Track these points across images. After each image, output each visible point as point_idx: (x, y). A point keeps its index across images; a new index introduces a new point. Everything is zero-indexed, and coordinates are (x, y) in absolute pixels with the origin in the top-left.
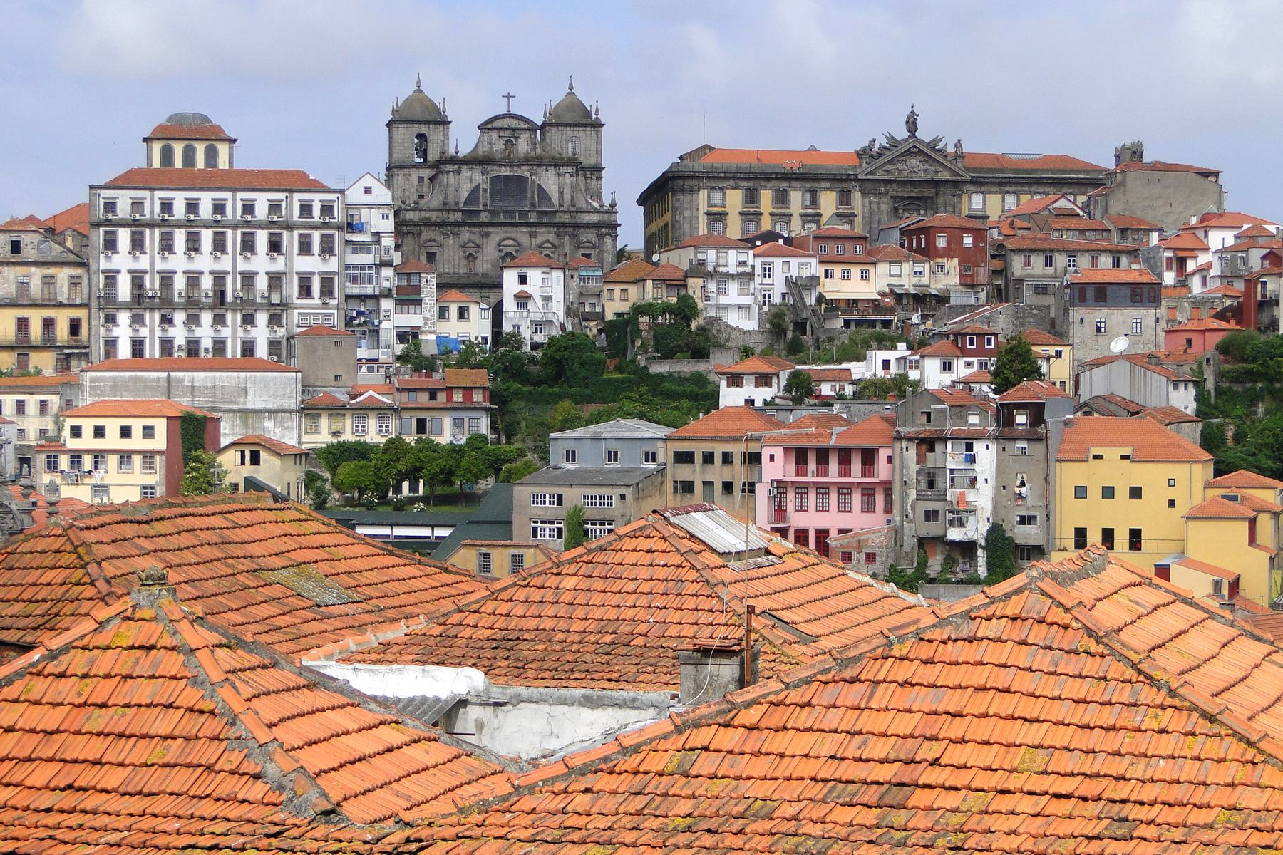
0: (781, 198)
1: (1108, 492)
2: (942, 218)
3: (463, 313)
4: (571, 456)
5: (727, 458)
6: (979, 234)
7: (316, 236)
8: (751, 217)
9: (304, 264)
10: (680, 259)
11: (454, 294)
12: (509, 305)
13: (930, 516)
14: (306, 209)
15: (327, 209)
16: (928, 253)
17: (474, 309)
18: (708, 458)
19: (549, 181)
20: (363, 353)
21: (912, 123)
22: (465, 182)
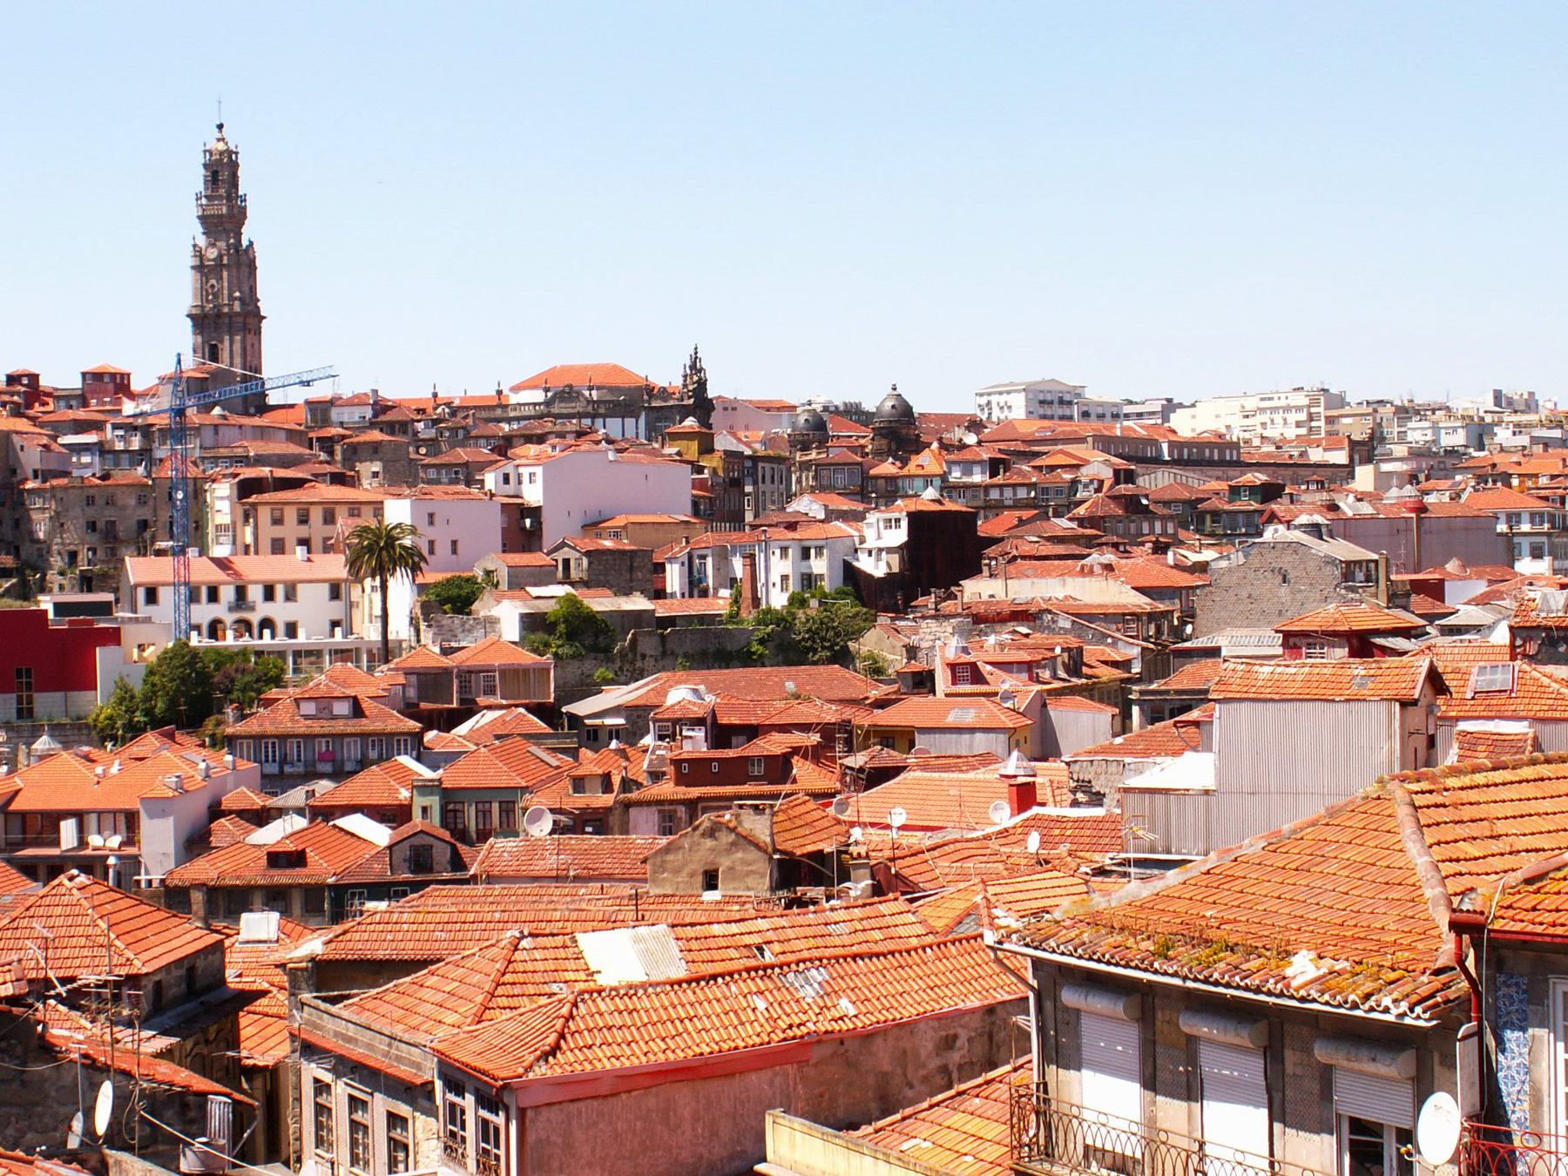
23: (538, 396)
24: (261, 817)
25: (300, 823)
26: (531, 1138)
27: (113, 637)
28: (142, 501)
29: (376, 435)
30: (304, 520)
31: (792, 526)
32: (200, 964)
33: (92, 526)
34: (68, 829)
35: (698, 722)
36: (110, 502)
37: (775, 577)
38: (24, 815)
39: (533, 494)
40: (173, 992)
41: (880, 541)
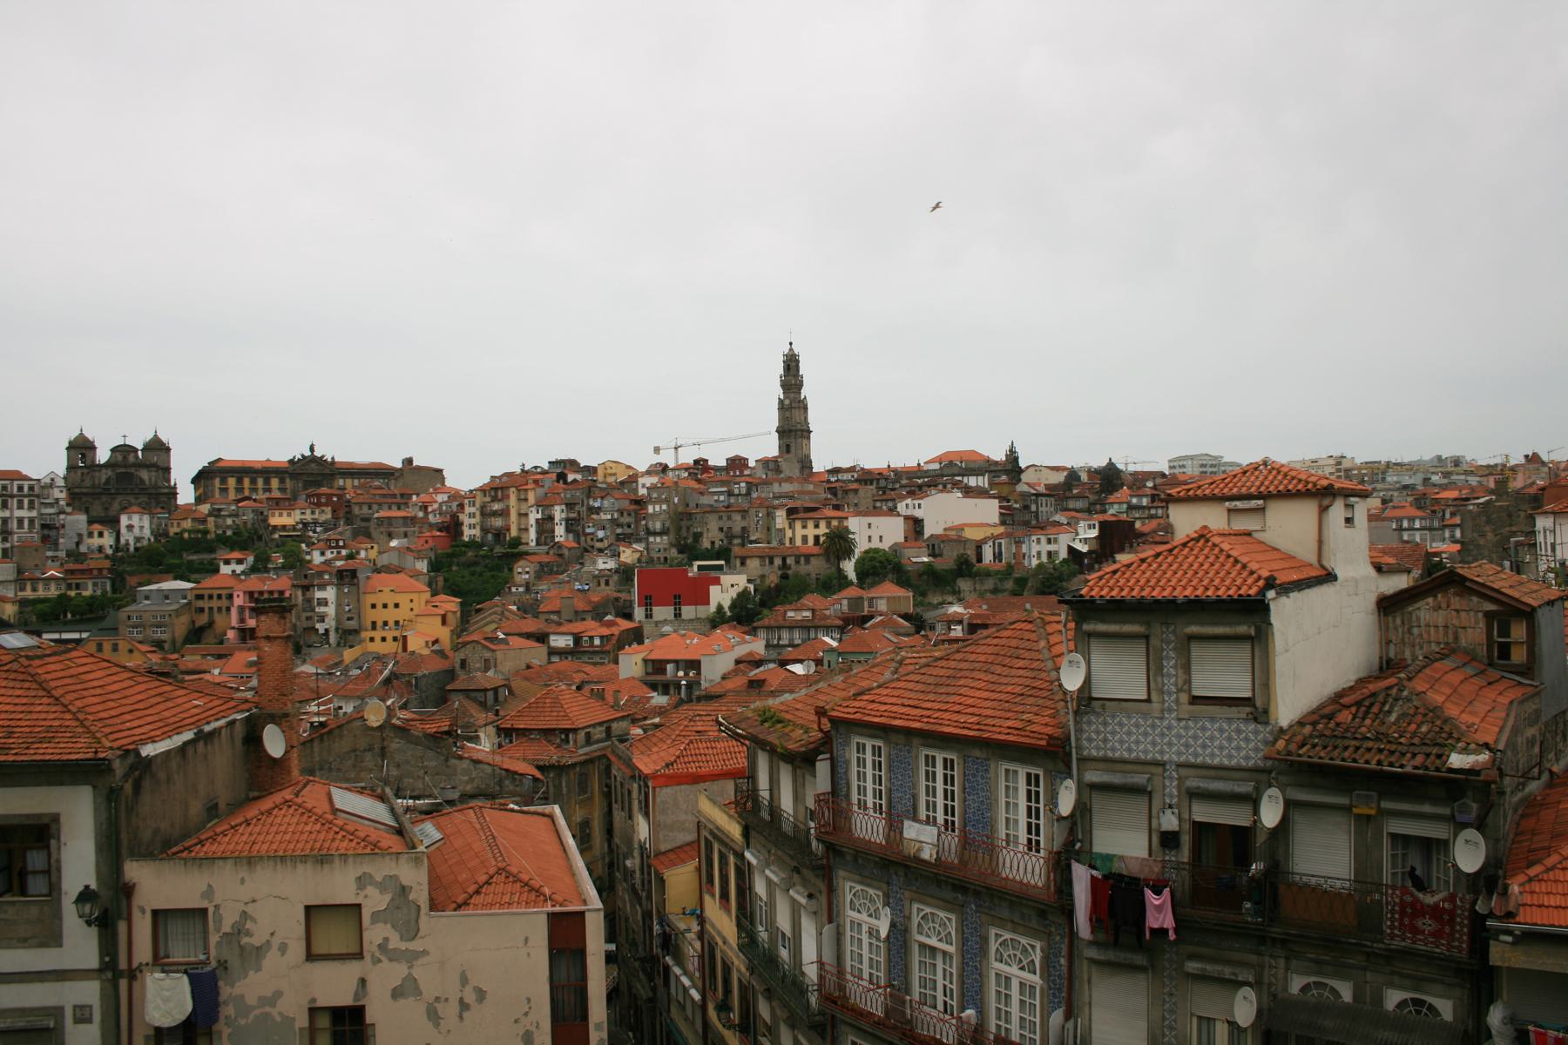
0: (253, 481)
1: (385, 606)
2: (324, 490)
3: (101, 535)
4: (147, 598)
5: (220, 597)
6: (340, 497)
7: (26, 501)
8: (239, 490)
9: (18, 513)
10: (205, 508)
11: (97, 527)
12: (123, 530)
13: (308, 618)
14: (20, 488)
15: (31, 488)
16: (319, 505)
17: (106, 533)
18: (211, 597)
19: (144, 475)
20: (49, 554)
21: (312, 449)
22: (104, 476)
23: (936, 466)
24: (759, 663)
25: (772, 666)
26: (658, 800)
27: (717, 581)
28: (744, 518)
29: (855, 486)
30: (817, 526)
31: (1042, 528)
32: (614, 725)
33: (721, 529)
34: (670, 667)
35: (960, 622)
36: (729, 518)
37: (1034, 552)
38: (653, 661)
39: (918, 513)
40: (598, 736)
41: (1086, 534)
